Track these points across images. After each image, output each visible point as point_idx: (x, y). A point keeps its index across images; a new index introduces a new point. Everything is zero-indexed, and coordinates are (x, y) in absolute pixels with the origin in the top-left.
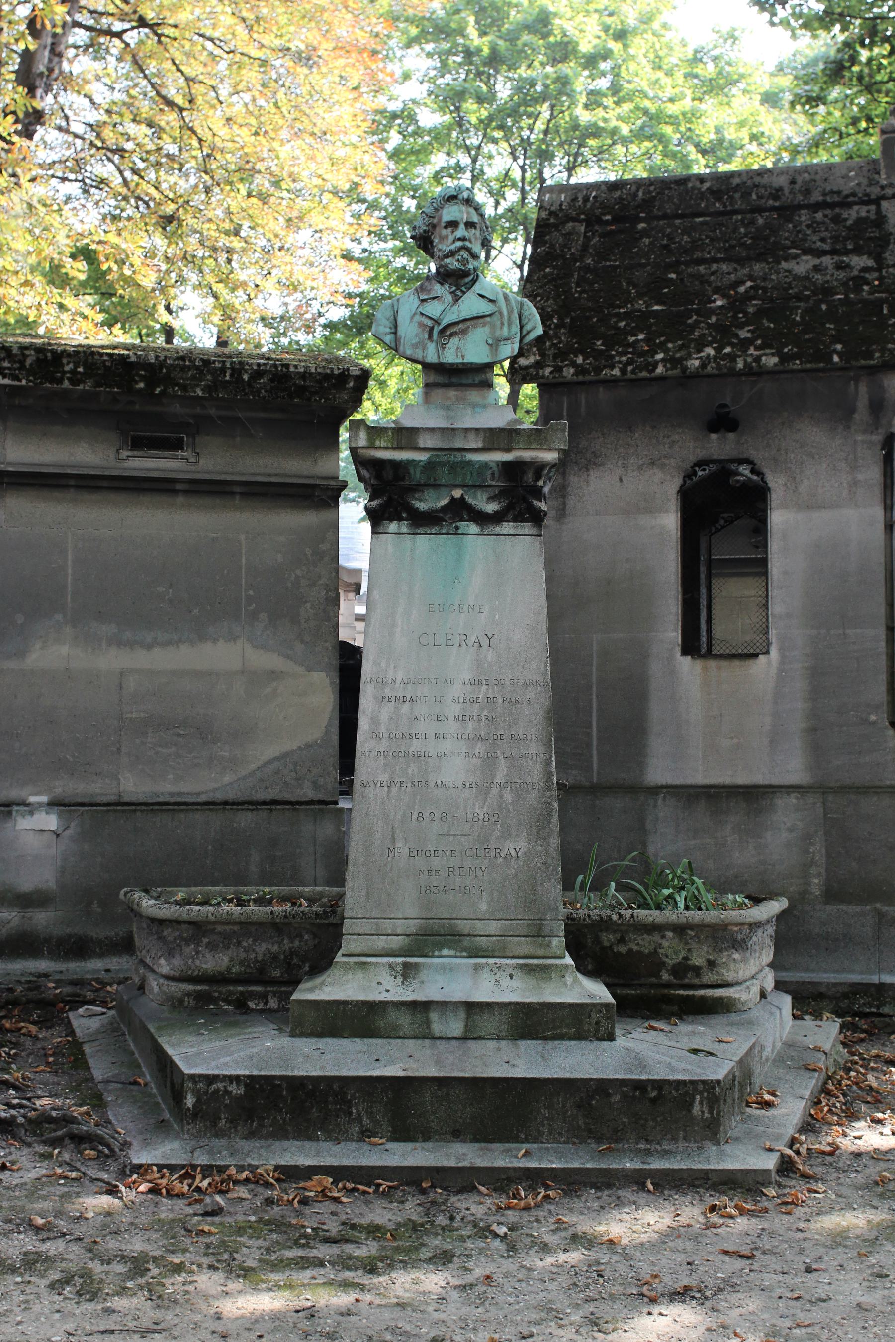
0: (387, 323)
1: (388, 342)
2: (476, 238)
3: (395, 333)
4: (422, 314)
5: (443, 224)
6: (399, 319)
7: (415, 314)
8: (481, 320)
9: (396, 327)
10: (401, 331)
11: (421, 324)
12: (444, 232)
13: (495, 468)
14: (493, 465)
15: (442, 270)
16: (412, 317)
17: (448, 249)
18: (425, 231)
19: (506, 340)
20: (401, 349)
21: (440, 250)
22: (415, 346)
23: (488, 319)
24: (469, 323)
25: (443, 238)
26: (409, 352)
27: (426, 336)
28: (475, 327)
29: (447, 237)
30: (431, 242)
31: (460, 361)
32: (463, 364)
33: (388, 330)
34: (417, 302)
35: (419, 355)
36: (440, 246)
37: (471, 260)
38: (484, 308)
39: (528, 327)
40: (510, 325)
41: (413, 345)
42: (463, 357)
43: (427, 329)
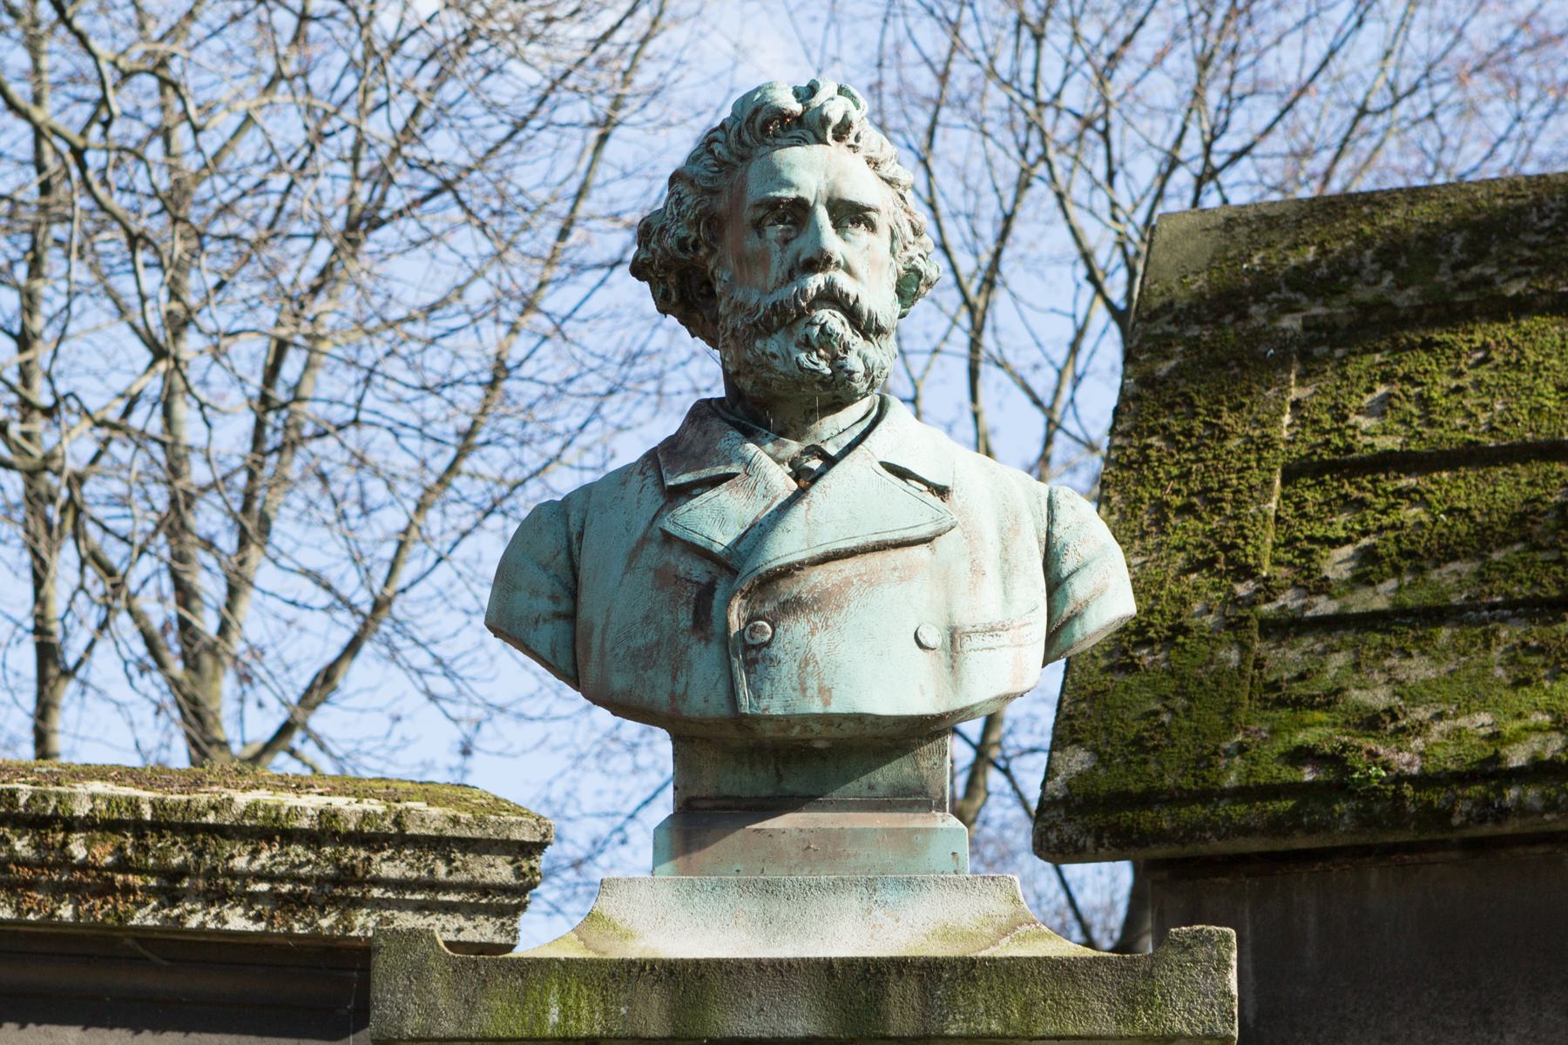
0: (545, 583)
1: (544, 650)
2: (872, 262)
3: (572, 616)
4: (668, 538)
5: (748, 215)
6: (586, 563)
7: (645, 540)
9: (574, 595)
10: (591, 608)
11: (665, 578)
12: (752, 243)
15: (746, 384)
16: (634, 555)
17: (769, 301)
18: (682, 244)
19: (991, 630)
20: (592, 672)
21: (739, 307)
22: (643, 658)
25: (749, 262)
26: (619, 682)
27: (685, 618)
28: (871, 582)
29: (763, 259)
30: (709, 284)
31: (817, 707)
32: (827, 719)
33: (544, 606)
34: (651, 499)
35: (659, 690)
36: (739, 295)
37: (857, 342)
38: (906, 511)
39: (1079, 589)
40: (1006, 577)
41: (635, 656)
42: (825, 693)
43: (691, 592)
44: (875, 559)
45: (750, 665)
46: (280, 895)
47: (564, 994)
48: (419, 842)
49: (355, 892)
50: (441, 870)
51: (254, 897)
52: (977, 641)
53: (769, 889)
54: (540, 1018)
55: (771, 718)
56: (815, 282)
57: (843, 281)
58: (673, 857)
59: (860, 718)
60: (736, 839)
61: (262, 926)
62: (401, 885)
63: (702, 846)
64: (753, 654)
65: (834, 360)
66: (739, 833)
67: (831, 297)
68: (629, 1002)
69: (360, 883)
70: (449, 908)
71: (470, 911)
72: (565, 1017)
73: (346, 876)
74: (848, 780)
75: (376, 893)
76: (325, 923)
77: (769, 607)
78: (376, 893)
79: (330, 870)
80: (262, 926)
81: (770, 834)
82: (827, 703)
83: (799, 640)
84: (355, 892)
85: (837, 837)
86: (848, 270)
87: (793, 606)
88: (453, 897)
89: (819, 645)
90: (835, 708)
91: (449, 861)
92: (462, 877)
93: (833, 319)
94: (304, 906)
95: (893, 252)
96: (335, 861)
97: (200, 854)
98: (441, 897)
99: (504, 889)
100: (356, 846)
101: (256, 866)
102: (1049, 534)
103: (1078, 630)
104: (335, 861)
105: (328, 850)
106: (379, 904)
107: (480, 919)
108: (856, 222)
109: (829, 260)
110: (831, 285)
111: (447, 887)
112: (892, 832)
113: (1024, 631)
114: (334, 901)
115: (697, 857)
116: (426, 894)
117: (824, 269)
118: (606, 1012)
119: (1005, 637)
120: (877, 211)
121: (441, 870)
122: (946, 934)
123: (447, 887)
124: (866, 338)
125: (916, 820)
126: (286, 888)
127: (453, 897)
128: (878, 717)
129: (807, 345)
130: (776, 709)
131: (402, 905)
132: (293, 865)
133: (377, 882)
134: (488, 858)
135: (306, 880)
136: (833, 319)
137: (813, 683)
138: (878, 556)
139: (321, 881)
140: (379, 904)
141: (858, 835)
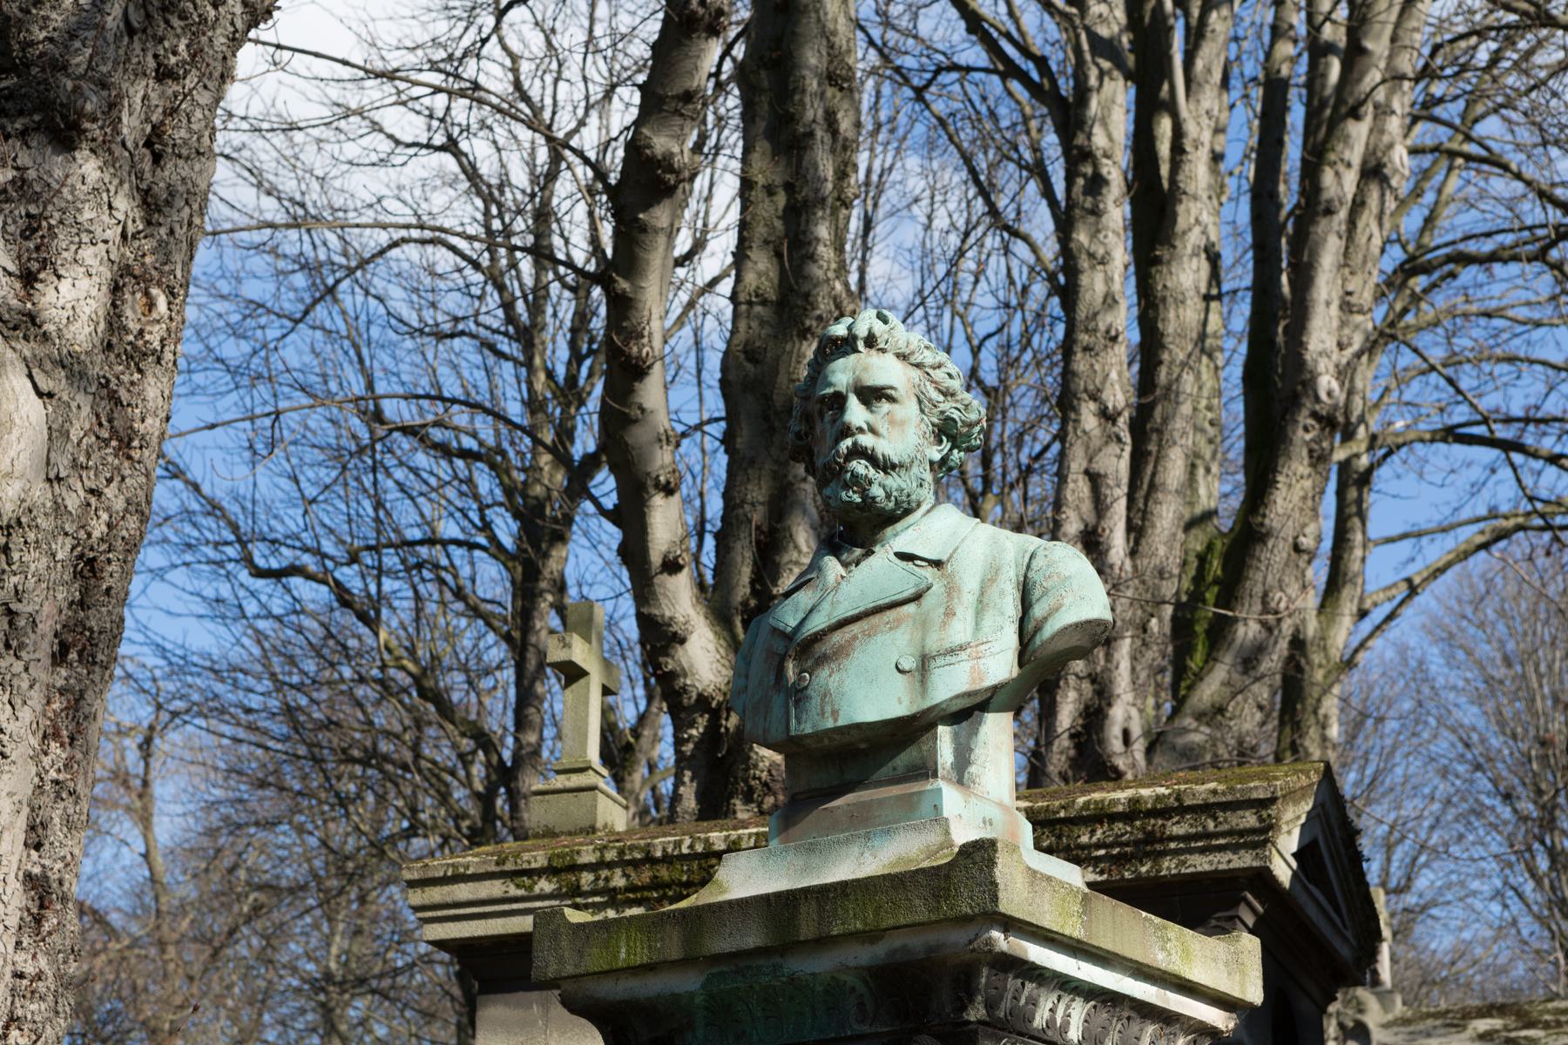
8: (891, 615)
13: (861, 988)
14: (850, 980)
23: (910, 608)
24: (855, 628)
28: (868, 635)
31: (830, 724)
42: (835, 714)
44: (875, 620)
45: (797, 702)
46: (1113, 856)
47: (628, 938)
48: (1193, 809)
49: (1158, 847)
50: (1211, 825)
51: (1098, 859)
52: (940, 661)
53: (811, 849)
54: (616, 957)
55: (807, 736)
56: (848, 442)
57: (866, 440)
58: (779, 834)
59: (859, 726)
60: (813, 816)
61: (1105, 876)
62: (1187, 838)
63: (795, 824)
64: (798, 695)
65: (864, 492)
66: (815, 813)
67: (858, 452)
68: (662, 939)
69: (1161, 841)
70: (1221, 848)
71: (1235, 848)
72: (628, 953)
73: (1150, 838)
74: (881, 766)
75: (1173, 845)
76: (1144, 869)
77: (810, 663)
78: (1173, 845)
79: (1140, 836)
80: (1105, 876)
81: (832, 810)
82: (836, 720)
83: (823, 682)
84: (1158, 847)
85: (866, 806)
86: (873, 430)
87: (823, 660)
88: (1222, 841)
89: (833, 682)
90: (840, 723)
91: (1215, 819)
92: (1225, 827)
93: (860, 467)
94: (1129, 860)
95: (922, 411)
96: (1143, 829)
97: (1059, 837)
98: (1214, 842)
99: (1253, 831)
100: (1155, 818)
101: (1094, 839)
102: (1026, 577)
103: (1038, 641)
104: (1143, 829)
105: (1138, 823)
106: (1176, 852)
107: (1242, 852)
108: (879, 398)
109: (849, 428)
110: (855, 444)
111: (1216, 835)
112: (899, 798)
113: (982, 647)
114: (1148, 855)
115: (793, 831)
116: (1204, 842)
117: (853, 435)
118: (650, 947)
119: (963, 655)
120: (892, 388)
121: (1211, 825)
122: (900, 860)
123: (1216, 835)
124: (886, 473)
125: (914, 787)
126: (1116, 851)
127: (1222, 841)
128: (869, 724)
129: (847, 487)
130: (808, 730)
131: (1191, 851)
132: (1118, 836)
133: (1172, 838)
134: (1240, 813)
135: (1127, 844)
136: (860, 467)
137: (828, 709)
138: (878, 616)
139: (1136, 843)
140: (1176, 852)
141: (881, 802)
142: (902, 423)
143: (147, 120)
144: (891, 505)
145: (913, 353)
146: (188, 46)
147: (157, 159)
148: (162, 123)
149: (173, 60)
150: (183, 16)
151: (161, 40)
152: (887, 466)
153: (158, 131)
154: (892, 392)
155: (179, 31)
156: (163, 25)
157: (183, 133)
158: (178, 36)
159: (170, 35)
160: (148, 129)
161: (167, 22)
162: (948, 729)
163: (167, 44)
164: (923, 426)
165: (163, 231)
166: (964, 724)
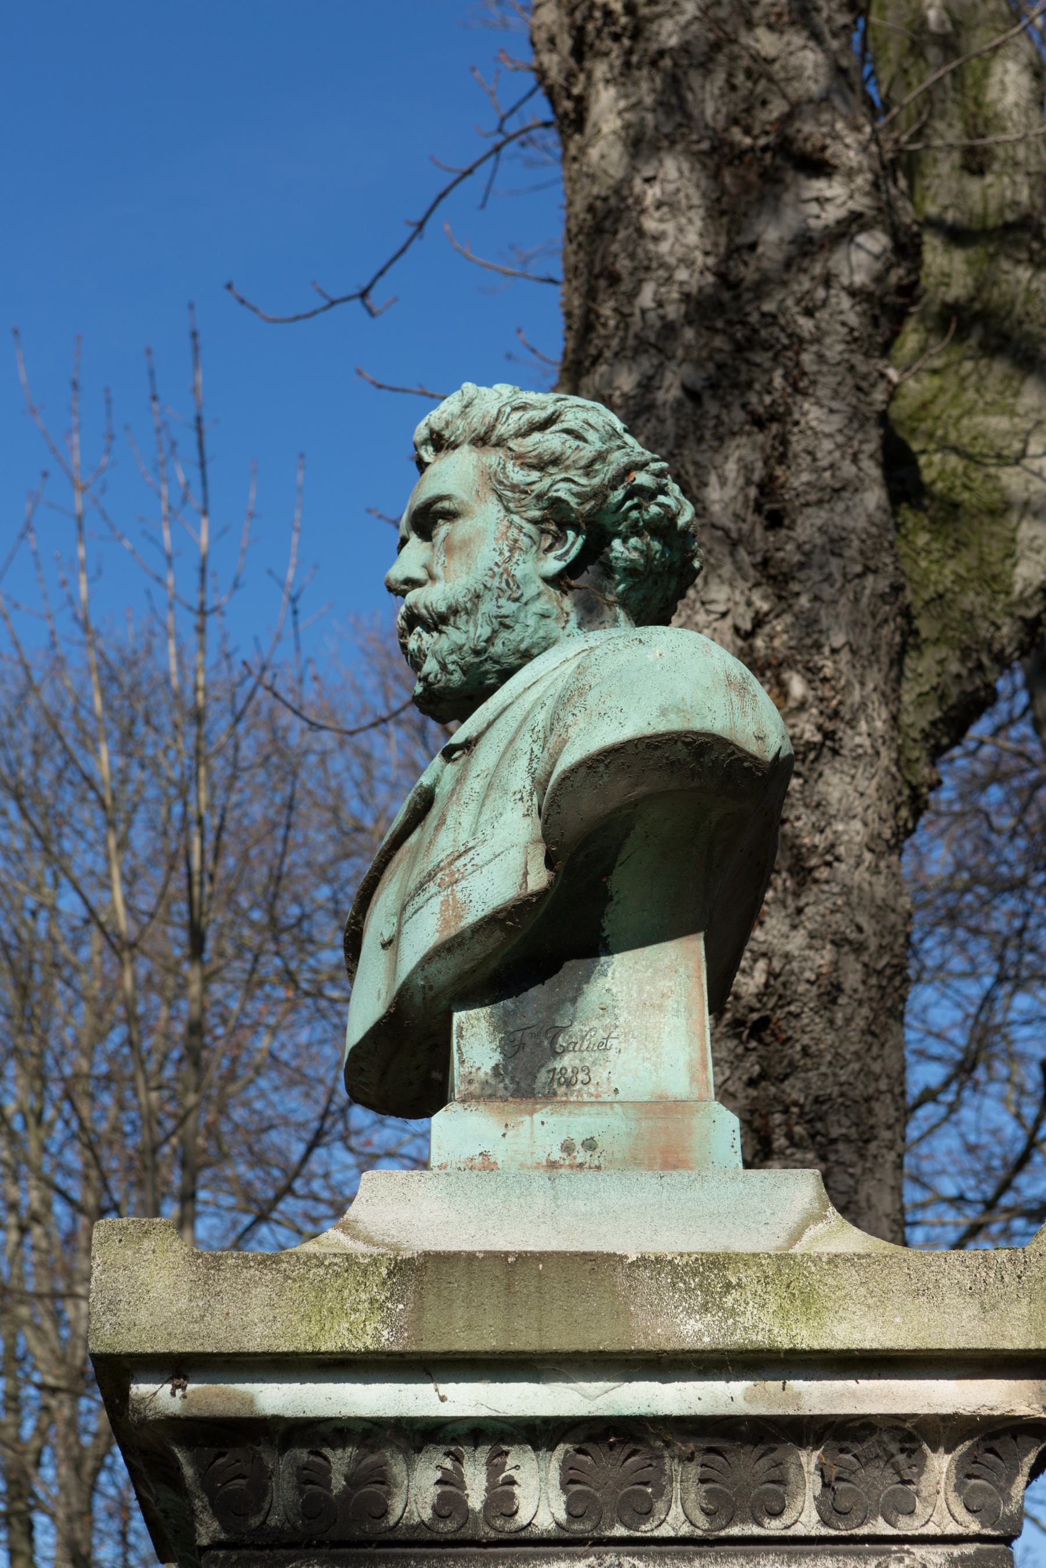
95: (508, 510)
120: (441, 498)
142: (466, 543)
143: (748, 482)
144: (457, 678)
145: (492, 428)
146: (785, 377)
147: (775, 520)
148: (771, 478)
149: (768, 399)
150: (766, 346)
151: (749, 385)
152: (437, 622)
153: (768, 487)
154: (446, 504)
155: (768, 364)
156: (744, 368)
157: (805, 477)
158: (769, 371)
159: (756, 373)
160: (753, 492)
161: (748, 362)
162: (483, 1012)
163: (757, 386)
164: (514, 532)
165: (804, 601)
166: (534, 992)
